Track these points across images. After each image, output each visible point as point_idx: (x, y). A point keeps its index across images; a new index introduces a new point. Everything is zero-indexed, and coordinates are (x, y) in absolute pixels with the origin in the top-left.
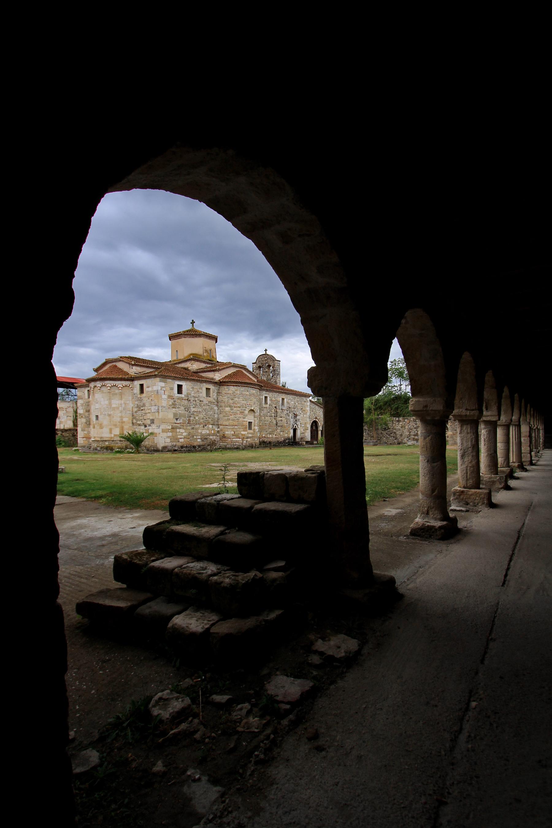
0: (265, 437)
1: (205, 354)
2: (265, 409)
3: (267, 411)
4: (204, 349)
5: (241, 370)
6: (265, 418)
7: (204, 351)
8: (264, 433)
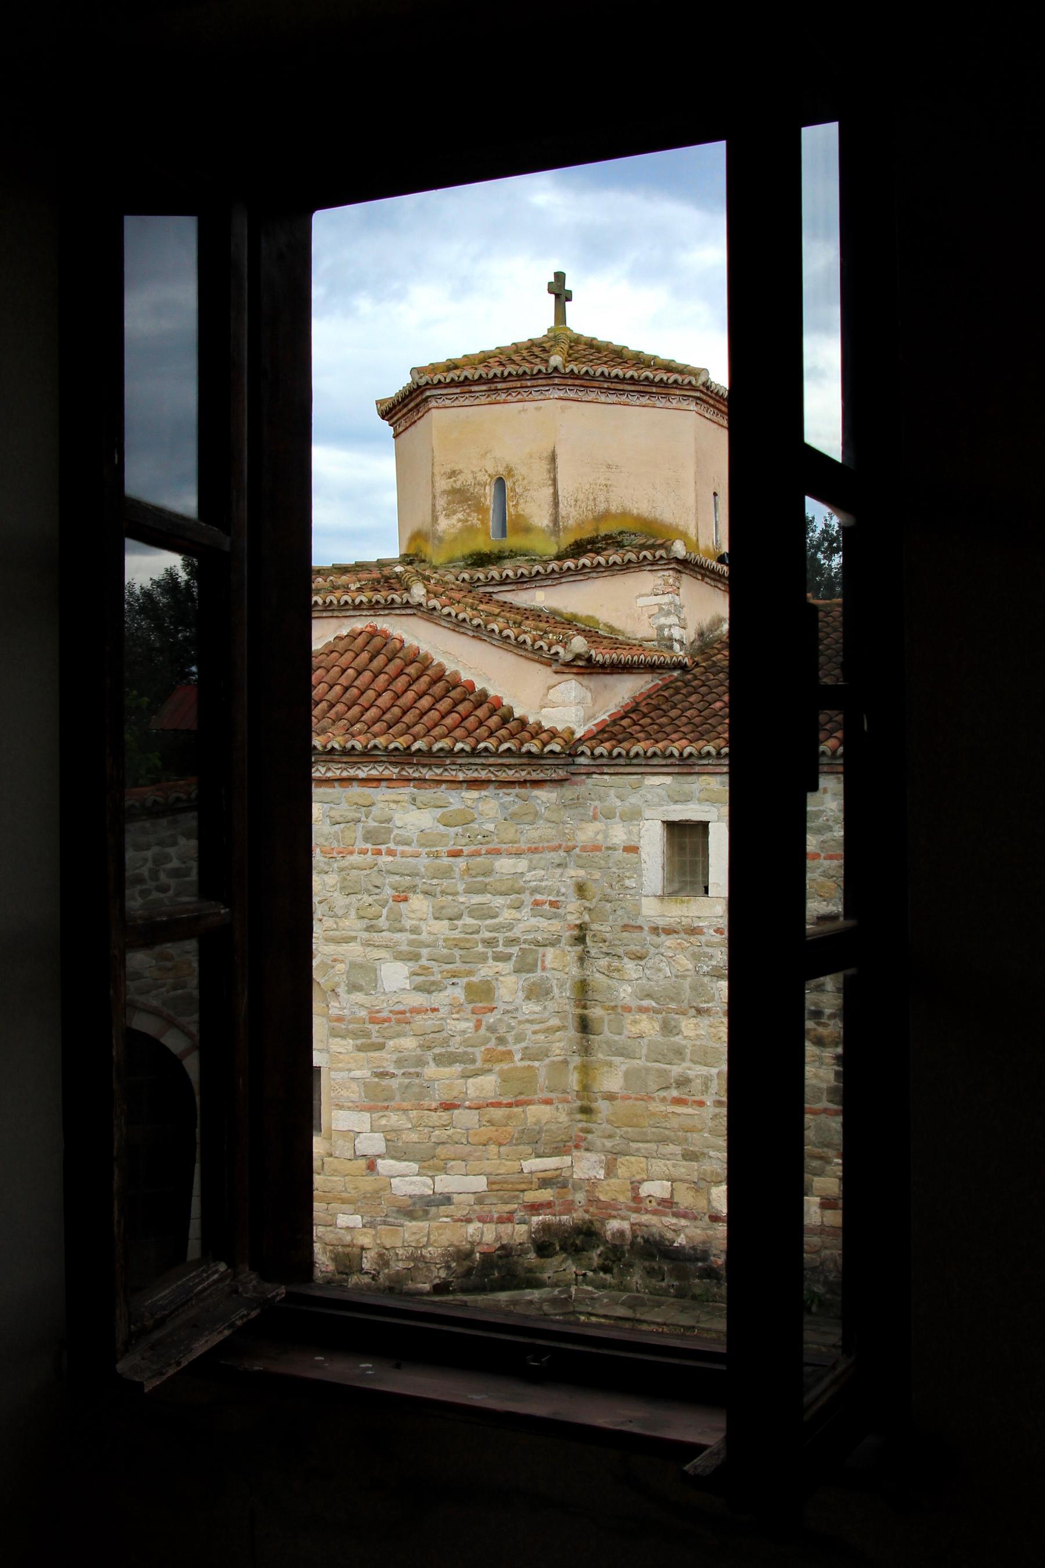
0: (667, 1204)
1: (444, 524)
2: (669, 941)
3: (696, 957)
4: (443, 484)
5: (384, 624)
6: (668, 1028)
7: (441, 502)
8: (658, 1166)
